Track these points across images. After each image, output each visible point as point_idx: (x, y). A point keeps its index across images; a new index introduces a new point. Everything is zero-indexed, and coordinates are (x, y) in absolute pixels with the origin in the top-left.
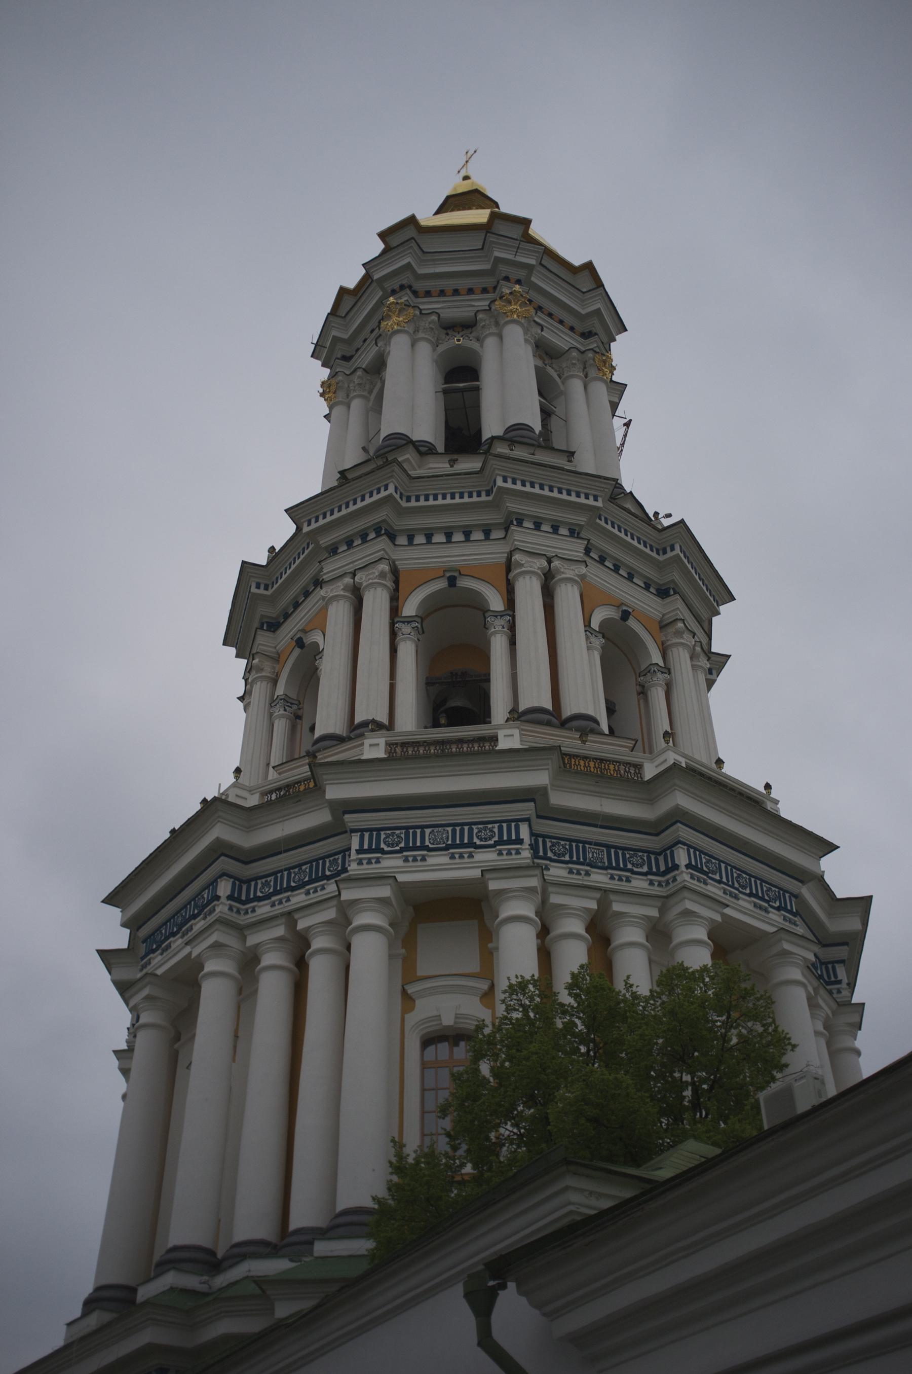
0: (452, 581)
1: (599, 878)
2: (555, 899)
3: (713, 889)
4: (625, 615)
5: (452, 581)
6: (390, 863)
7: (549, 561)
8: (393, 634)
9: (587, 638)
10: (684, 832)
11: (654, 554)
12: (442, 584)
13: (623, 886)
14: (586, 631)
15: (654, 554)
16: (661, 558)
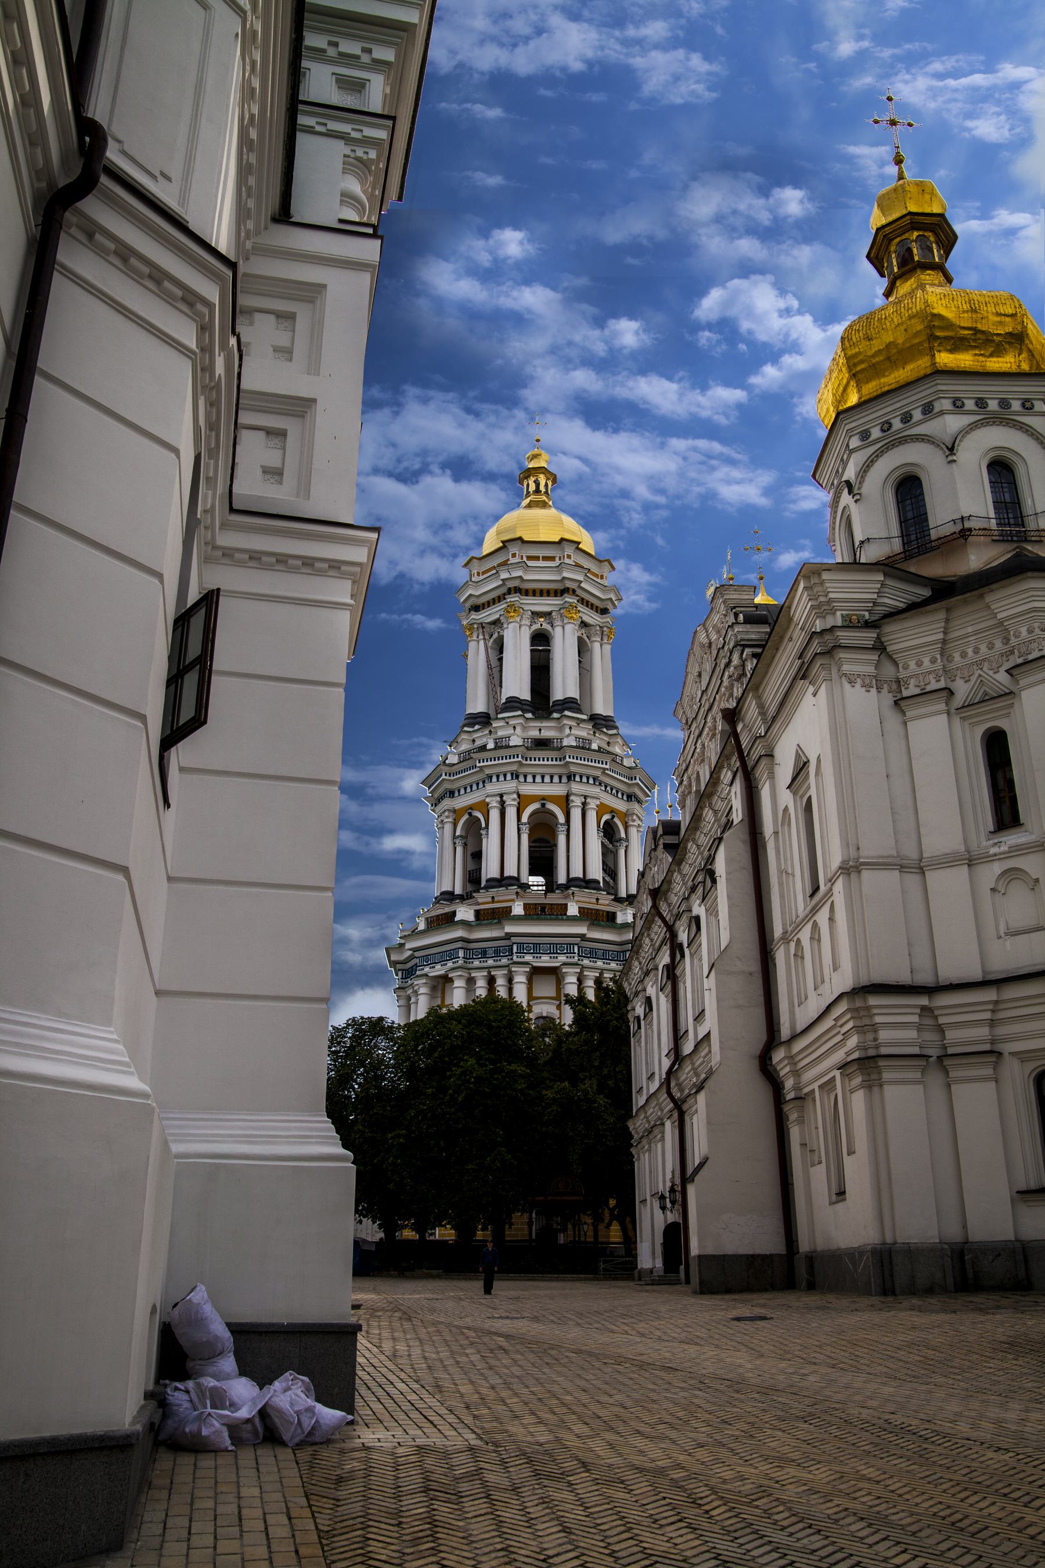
0: (470, 814)
1: (490, 962)
2: (473, 975)
3: (528, 958)
4: (543, 805)
5: (470, 814)
6: (427, 969)
7: (501, 796)
8: (455, 843)
9: (519, 830)
10: (514, 939)
11: (558, 763)
12: (466, 816)
13: (499, 963)
14: (518, 825)
15: (558, 763)
16: (562, 763)
